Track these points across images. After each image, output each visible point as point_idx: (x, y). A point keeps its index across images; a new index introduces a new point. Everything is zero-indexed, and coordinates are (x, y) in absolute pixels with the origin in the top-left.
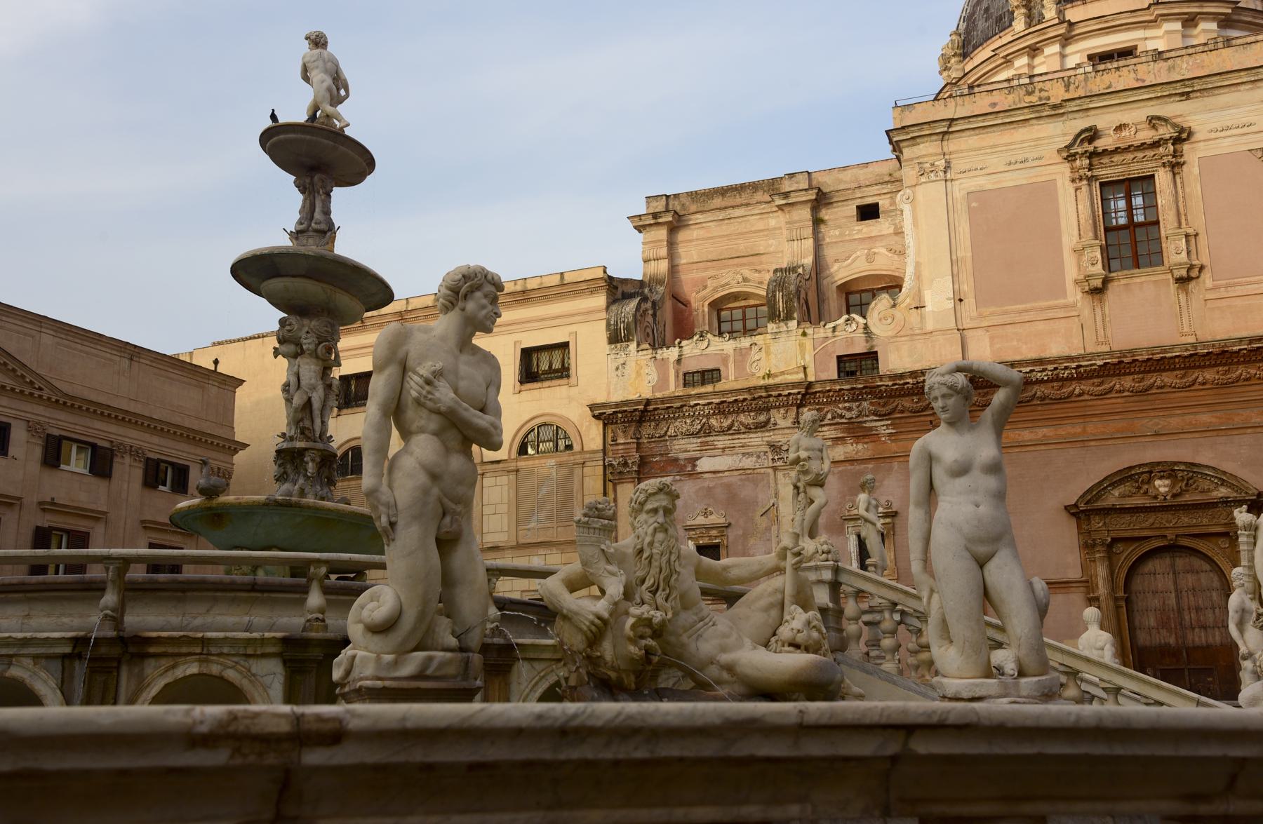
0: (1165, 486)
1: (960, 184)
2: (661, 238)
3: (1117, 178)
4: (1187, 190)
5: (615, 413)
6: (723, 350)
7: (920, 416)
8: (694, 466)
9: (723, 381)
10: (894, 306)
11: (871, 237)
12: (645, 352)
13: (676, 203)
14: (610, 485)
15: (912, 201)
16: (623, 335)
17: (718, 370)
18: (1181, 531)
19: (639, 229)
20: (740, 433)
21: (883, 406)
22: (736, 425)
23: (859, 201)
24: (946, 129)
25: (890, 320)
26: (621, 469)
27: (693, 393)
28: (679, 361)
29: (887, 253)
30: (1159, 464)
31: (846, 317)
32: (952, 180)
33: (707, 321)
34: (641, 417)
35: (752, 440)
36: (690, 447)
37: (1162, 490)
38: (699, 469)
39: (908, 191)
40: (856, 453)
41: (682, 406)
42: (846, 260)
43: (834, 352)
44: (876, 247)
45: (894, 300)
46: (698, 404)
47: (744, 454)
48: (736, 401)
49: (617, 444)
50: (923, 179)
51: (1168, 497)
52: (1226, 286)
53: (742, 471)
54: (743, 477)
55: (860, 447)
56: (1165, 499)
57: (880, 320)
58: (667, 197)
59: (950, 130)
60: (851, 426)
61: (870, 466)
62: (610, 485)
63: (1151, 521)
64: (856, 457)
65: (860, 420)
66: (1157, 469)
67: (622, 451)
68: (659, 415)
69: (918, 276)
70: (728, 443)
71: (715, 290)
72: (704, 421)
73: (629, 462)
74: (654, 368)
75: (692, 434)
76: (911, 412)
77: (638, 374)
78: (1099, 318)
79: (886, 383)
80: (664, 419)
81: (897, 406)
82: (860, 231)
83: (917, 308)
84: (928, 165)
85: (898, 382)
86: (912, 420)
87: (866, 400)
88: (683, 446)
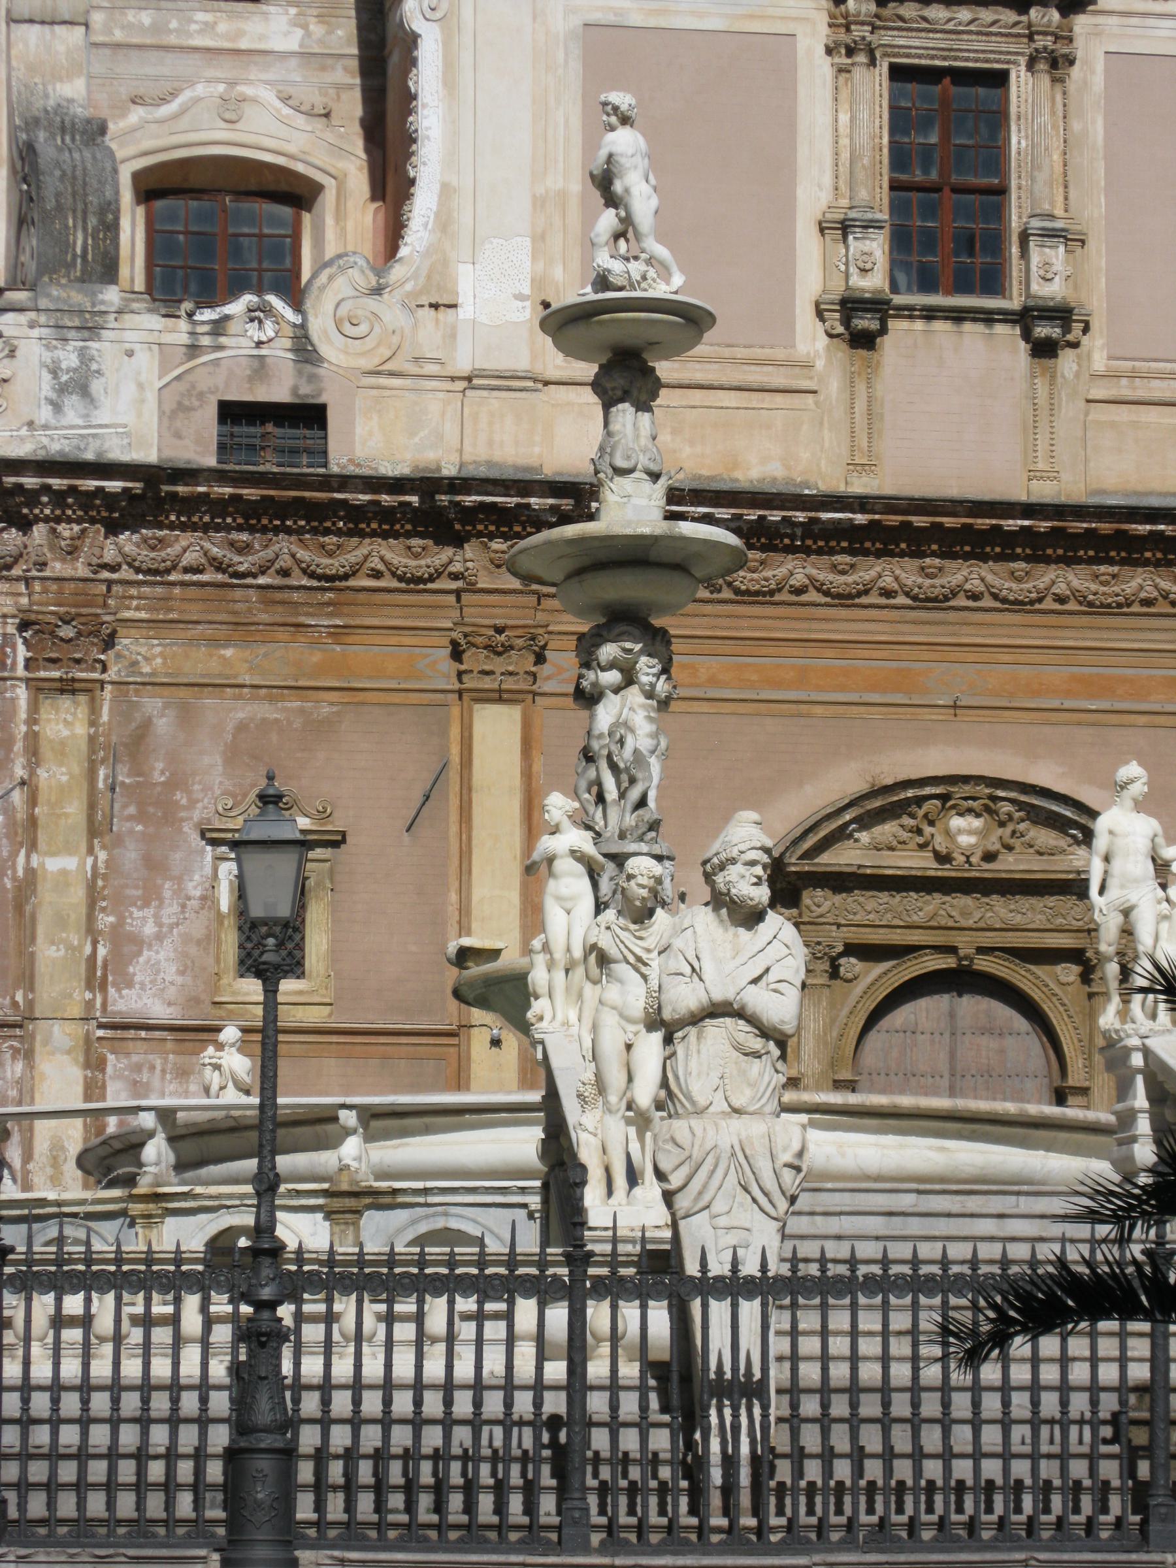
0: (970, 832)
3: (923, 62)
4: (1076, 126)
7: (426, 591)
10: (378, 291)
18: (988, 940)
21: (330, 554)
25: (362, 329)
29: (278, 104)
30: (966, 779)
37: (965, 840)
42: (164, 100)
44: (248, 82)
51: (974, 860)
52: (1133, 376)
56: (968, 862)
63: (930, 908)
66: (967, 790)
69: (444, 222)
76: (401, 579)
78: (860, 406)
82: (209, 27)
83: (435, 306)
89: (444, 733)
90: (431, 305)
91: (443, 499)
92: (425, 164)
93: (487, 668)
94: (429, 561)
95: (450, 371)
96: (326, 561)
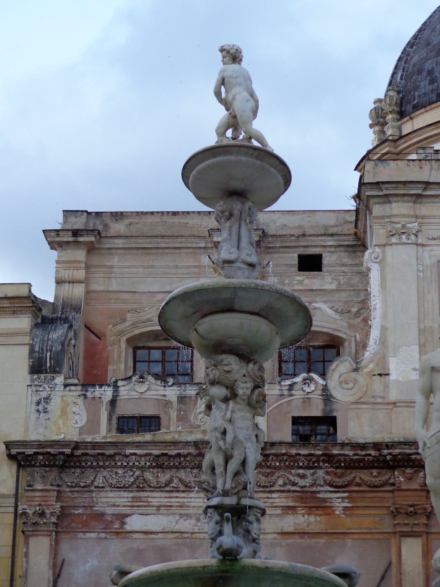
1: (431, 250)
2: (78, 258)
5: (36, 454)
6: (164, 396)
7: (379, 491)
8: (123, 523)
9: (163, 430)
10: (356, 370)
11: (312, 290)
12: (73, 388)
13: (98, 222)
14: (20, 537)
15: (382, 262)
16: (48, 364)
17: (157, 418)
19: (53, 245)
20: (178, 491)
21: (339, 477)
22: (175, 481)
23: (302, 249)
24: (420, 192)
25: (351, 385)
26: (37, 519)
27: (128, 440)
28: (113, 402)
31: (304, 375)
32: (423, 245)
33: (123, 359)
34: (65, 462)
35: (192, 500)
36: (118, 501)
38: (128, 528)
39: (377, 249)
40: (308, 525)
41: (115, 454)
43: (289, 412)
44: (316, 302)
45: (357, 363)
46: (135, 454)
47: (181, 515)
48: (179, 455)
49: (33, 490)
50: (394, 240)
53: (178, 534)
54: (179, 541)
55: (312, 519)
57: (341, 383)
58: (89, 213)
59: (425, 193)
60: (303, 495)
61: (322, 541)
62: (20, 537)
64: (307, 530)
65: (314, 489)
67: (38, 499)
68: (86, 461)
70: (164, 501)
71: (135, 325)
72: (138, 473)
73: (47, 511)
74: (82, 407)
75: (124, 487)
76: (369, 486)
77: (64, 413)
79: (347, 453)
80: (92, 467)
81: (355, 478)
82: (301, 282)
83: (380, 375)
84: (399, 226)
85: (359, 452)
86: (370, 495)
87: (320, 468)
88: (112, 500)
89: (389, 550)
90: (378, 374)
91: (385, 452)
92: (374, 319)
93: (406, 522)
94: (380, 478)
95: (386, 401)
96: (338, 480)
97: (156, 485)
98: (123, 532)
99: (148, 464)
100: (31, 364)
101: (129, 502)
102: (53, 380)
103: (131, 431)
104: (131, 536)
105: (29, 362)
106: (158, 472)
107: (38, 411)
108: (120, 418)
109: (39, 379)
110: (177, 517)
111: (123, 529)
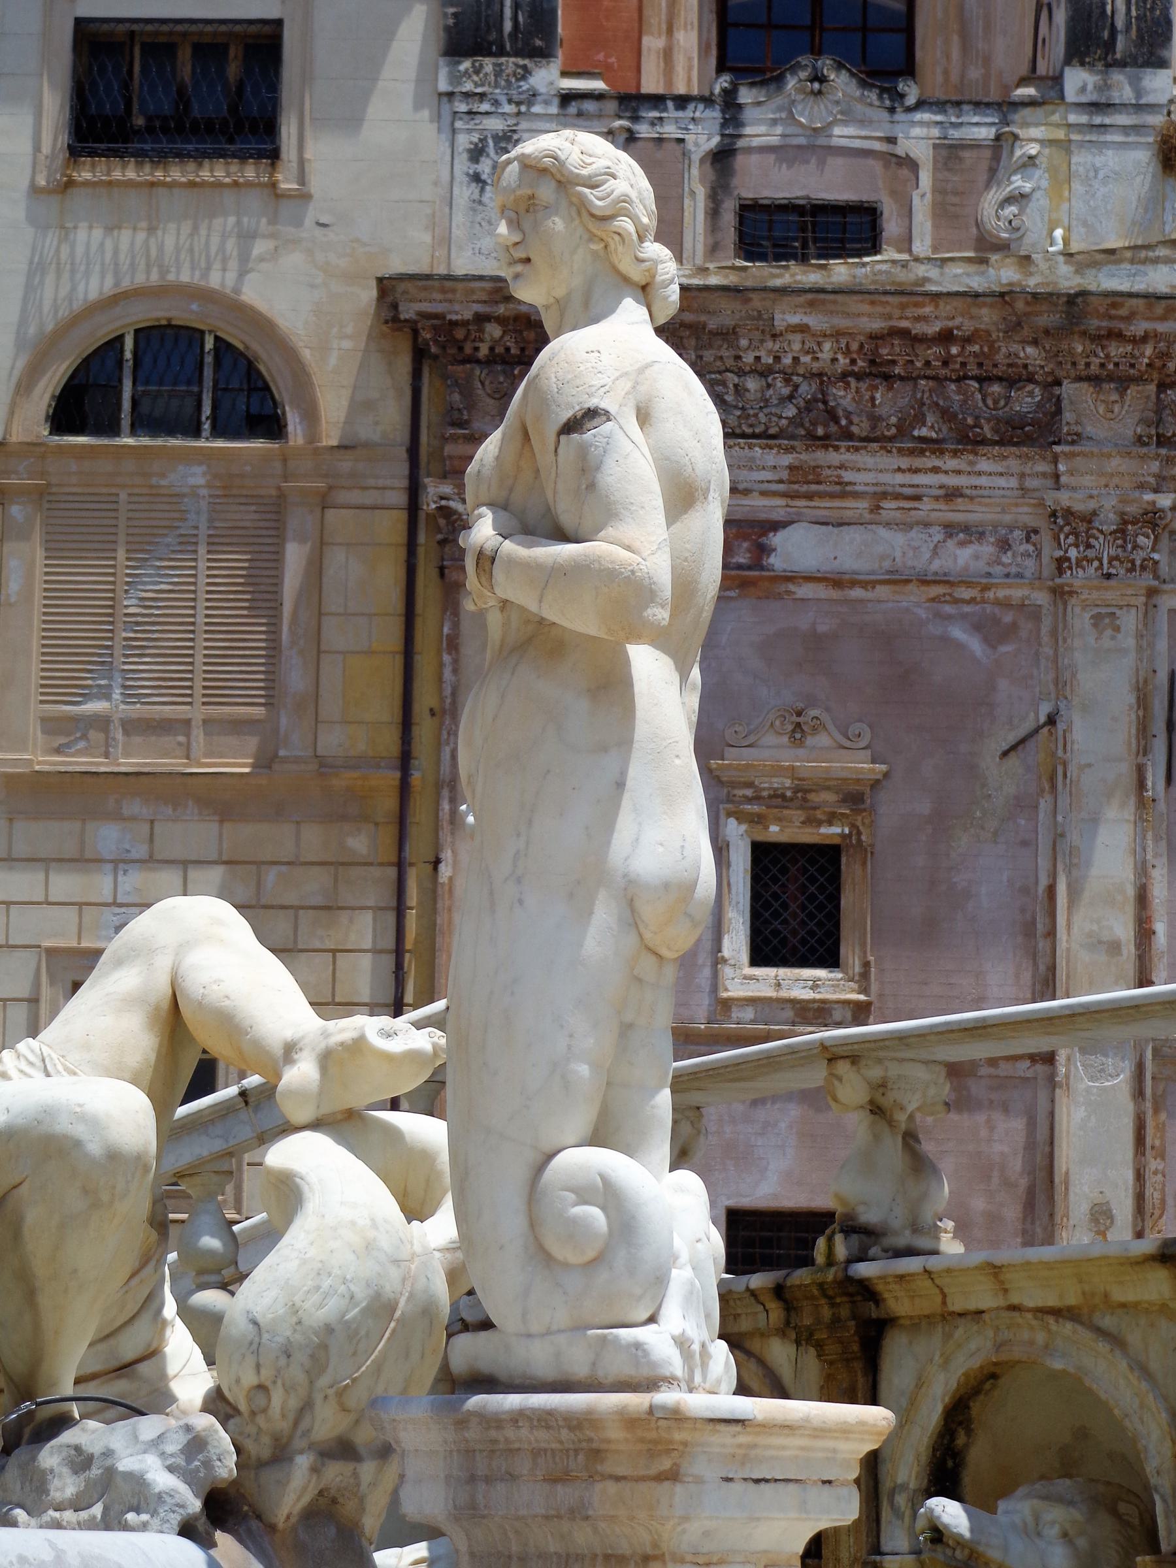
6: (892, 140)
16: (508, 26)
28: (722, 158)
38: (776, 562)
47: (950, 529)
75: (764, 435)
97: (866, 425)
98: (761, 578)
99: (843, 361)
100: (451, 22)
101: (781, 481)
102: (524, 78)
103: (782, 253)
104: (789, 592)
105: (445, 15)
106: (876, 388)
107: (477, 178)
108: (749, 210)
109: (477, 72)
110: (938, 534)
111: (762, 568)
